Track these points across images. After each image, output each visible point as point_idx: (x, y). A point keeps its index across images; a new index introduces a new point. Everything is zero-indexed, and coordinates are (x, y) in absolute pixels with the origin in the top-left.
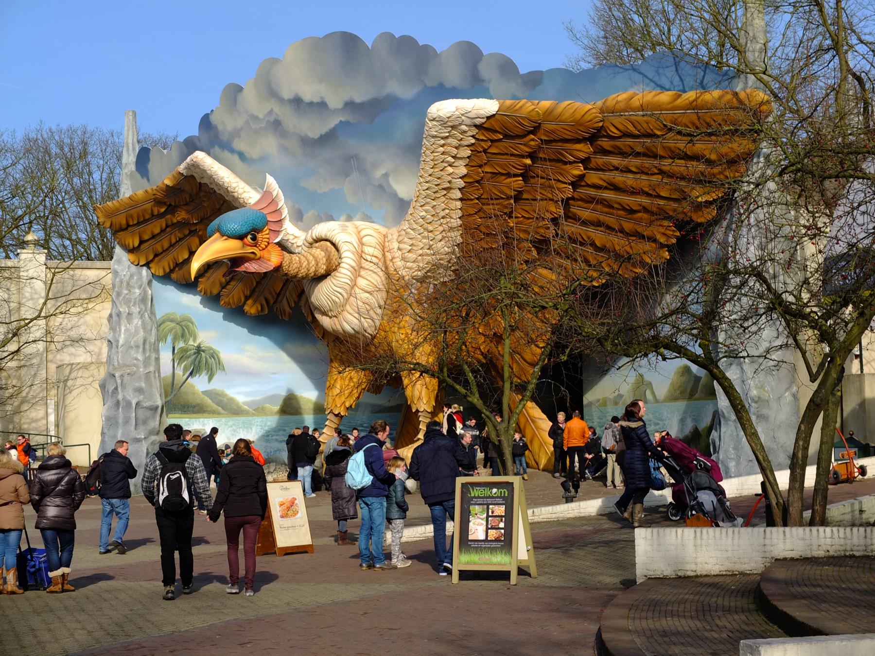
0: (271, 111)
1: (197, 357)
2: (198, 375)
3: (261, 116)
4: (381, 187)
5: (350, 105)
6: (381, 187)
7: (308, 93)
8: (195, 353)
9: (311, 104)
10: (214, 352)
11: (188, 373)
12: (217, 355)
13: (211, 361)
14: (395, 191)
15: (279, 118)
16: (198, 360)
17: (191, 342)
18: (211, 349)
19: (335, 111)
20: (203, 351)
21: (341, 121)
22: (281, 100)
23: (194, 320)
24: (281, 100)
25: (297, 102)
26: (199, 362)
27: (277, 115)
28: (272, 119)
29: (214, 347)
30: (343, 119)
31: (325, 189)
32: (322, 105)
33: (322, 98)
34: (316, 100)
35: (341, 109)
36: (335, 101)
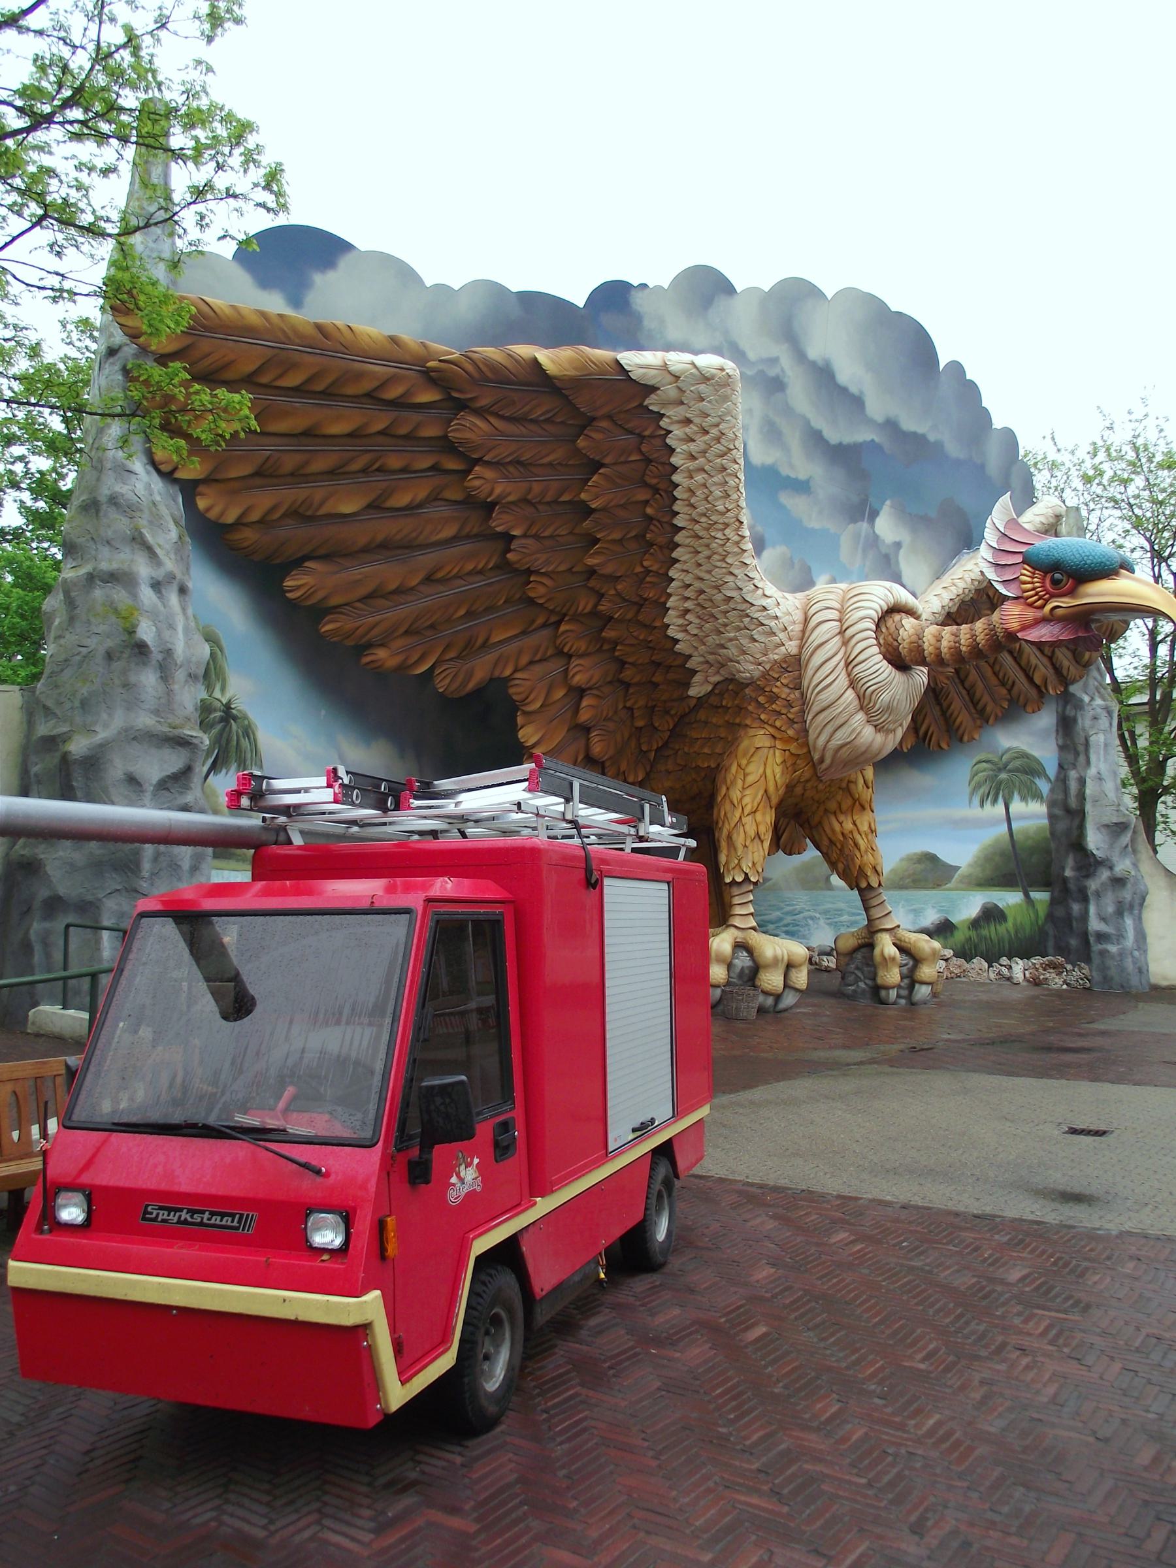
0: (774, 361)
1: (224, 729)
2: (224, 771)
3: (752, 355)
4: (887, 557)
5: (891, 426)
6: (887, 557)
7: (848, 372)
8: (222, 720)
9: (844, 390)
10: (249, 725)
11: (211, 761)
12: (254, 735)
13: (245, 743)
14: (901, 572)
15: (786, 380)
16: (225, 735)
17: (217, 694)
18: (246, 717)
19: (870, 422)
20: (235, 718)
21: (873, 441)
22: (800, 355)
23: (224, 643)
24: (800, 355)
25: (823, 375)
26: (228, 741)
27: (783, 370)
28: (772, 372)
29: (251, 715)
30: (877, 439)
31: (814, 524)
32: (857, 402)
33: (861, 392)
34: (854, 389)
35: (879, 424)
36: (876, 408)
